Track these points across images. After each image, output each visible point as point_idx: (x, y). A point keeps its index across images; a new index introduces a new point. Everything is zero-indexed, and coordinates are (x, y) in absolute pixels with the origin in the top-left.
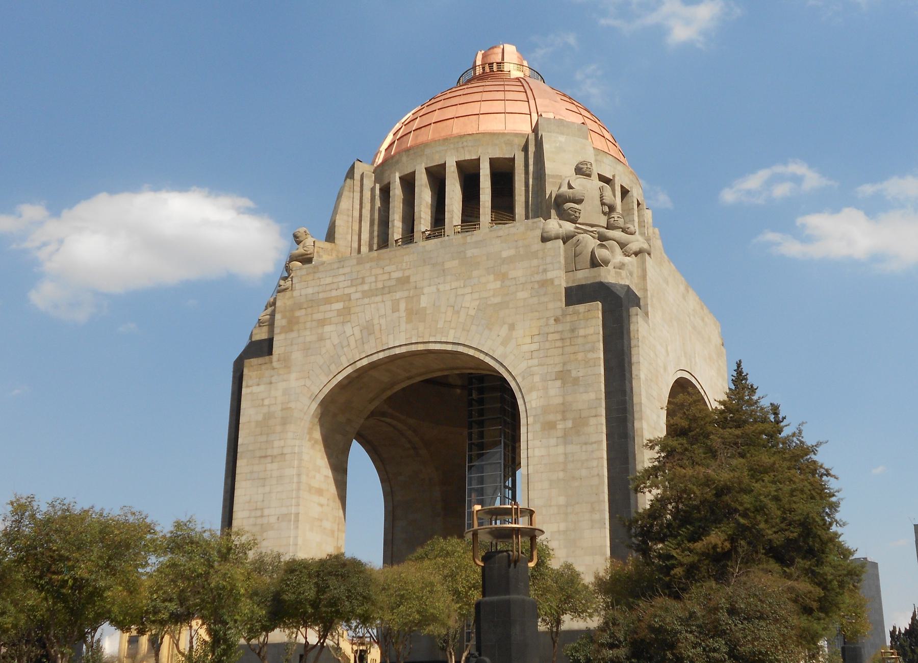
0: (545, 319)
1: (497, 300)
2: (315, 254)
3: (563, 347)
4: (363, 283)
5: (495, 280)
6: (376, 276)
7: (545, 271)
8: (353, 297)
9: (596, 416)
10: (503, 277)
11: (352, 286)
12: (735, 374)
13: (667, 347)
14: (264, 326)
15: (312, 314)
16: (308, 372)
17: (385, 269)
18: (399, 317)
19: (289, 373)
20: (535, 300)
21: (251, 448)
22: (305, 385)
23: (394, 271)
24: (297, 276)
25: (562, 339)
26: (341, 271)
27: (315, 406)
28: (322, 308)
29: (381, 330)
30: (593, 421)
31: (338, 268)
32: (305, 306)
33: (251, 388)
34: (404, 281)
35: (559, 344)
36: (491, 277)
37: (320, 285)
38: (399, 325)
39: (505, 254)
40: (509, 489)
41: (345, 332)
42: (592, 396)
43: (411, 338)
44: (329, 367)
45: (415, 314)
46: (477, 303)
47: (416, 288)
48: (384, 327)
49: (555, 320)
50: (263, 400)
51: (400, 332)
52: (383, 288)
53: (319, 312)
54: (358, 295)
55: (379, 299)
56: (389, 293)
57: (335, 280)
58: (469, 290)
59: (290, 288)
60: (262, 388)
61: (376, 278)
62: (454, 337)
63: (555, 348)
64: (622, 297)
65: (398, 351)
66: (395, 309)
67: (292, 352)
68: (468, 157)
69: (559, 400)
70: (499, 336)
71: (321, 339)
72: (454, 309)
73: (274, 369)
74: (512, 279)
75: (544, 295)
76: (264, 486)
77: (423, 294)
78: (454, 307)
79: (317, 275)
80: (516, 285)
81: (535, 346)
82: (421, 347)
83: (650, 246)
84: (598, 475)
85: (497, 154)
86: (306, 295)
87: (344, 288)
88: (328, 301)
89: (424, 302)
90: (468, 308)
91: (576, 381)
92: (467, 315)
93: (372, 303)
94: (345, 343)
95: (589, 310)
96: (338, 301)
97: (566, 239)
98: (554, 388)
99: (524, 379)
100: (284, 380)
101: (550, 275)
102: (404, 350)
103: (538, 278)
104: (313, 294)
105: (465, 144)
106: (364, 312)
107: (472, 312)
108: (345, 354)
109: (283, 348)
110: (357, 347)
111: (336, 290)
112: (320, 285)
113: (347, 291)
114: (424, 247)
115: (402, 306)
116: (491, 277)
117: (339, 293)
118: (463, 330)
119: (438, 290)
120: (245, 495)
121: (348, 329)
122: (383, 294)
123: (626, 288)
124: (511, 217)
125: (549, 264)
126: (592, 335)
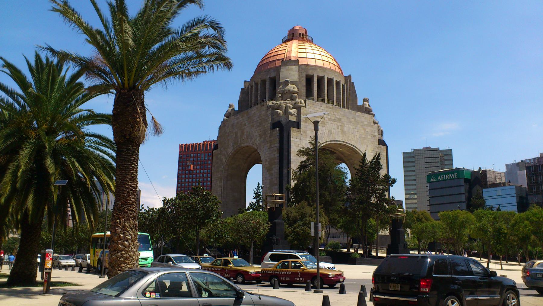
5: (363, 130)
10: (365, 130)
17: (335, 113)
18: (339, 131)
19: (307, 138)
20: (372, 140)
21: (295, 161)
26: (321, 108)
34: (340, 120)
45: (343, 132)
50: (298, 145)
52: (334, 119)
55: (333, 122)
73: (301, 134)
75: (374, 139)
79: (314, 106)
89: (346, 129)
94: (324, 134)
107: (358, 138)
112: (315, 110)
115: (340, 128)
116: (362, 129)
118: (356, 142)
119: (349, 127)
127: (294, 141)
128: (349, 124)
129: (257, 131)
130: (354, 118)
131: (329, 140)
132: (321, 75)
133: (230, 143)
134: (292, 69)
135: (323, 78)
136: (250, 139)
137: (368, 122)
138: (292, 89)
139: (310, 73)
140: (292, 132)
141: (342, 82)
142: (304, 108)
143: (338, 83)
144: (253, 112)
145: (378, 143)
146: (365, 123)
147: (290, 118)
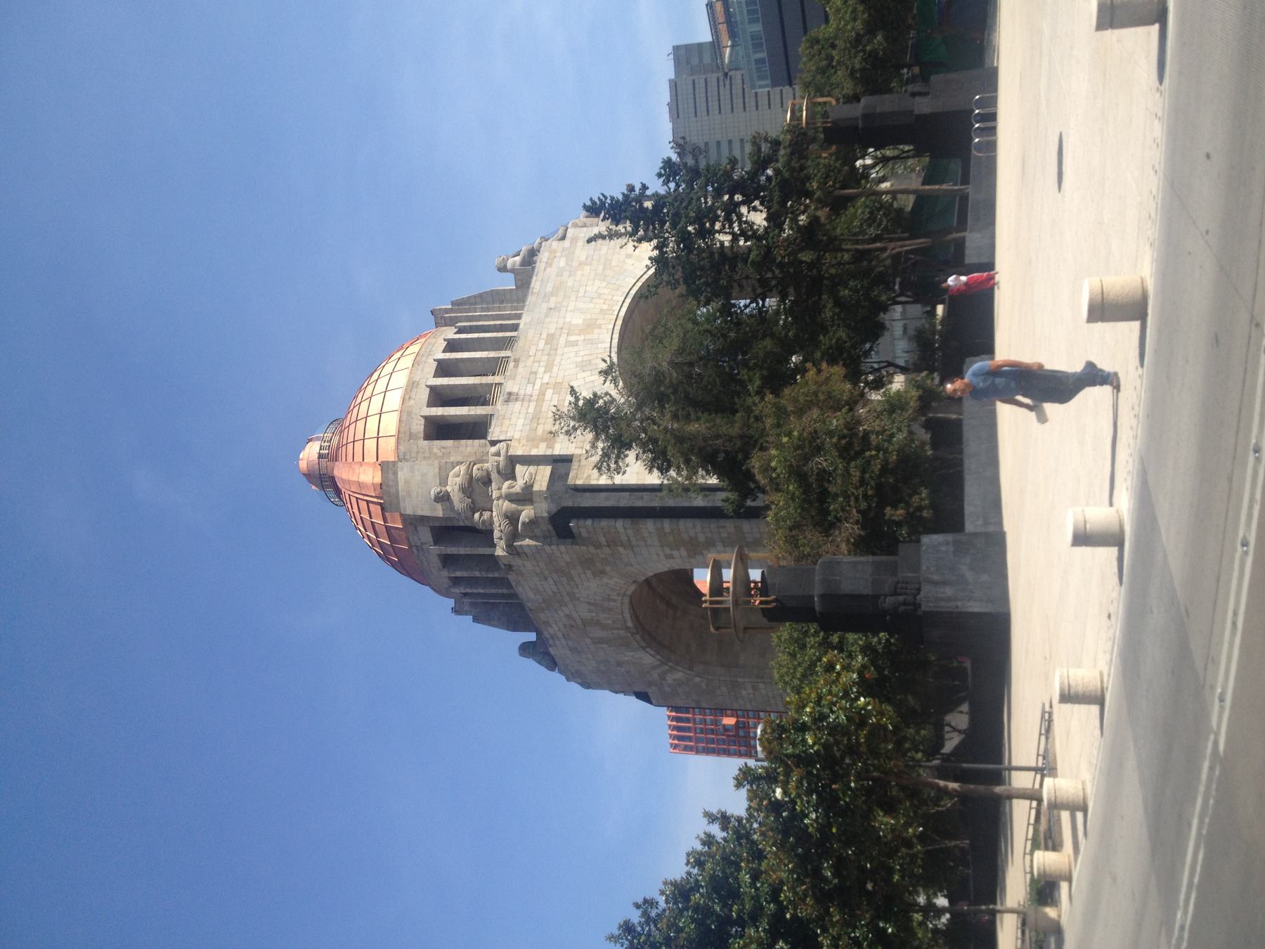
4: (535, 373)
8: (546, 379)
28: (544, 409)
37: (520, 413)
47: (562, 328)
48: (588, 352)
52: (549, 354)
55: (558, 359)
58: (582, 290)
59: (509, 442)
61: (537, 362)
65: (615, 341)
82: (619, 322)
96: (544, 395)
102: (616, 336)
107: (604, 284)
112: (520, 413)
113: (537, 386)
118: (617, 290)
119: (572, 311)
128: (563, 312)
129: (585, 583)
130: (547, 297)
132: (424, 394)
133: (626, 659)
134: (407, 482)
135: (434, 390)
136: (611, 603)
137: (561, 256)
138: (458, 480)
139: (419, 426)
140: (579, 482)
141: (450, 333)
142: (512, 443)
143: (452, 346)
144: (531, 595)
146: (562, 263)
147: (541, 486)
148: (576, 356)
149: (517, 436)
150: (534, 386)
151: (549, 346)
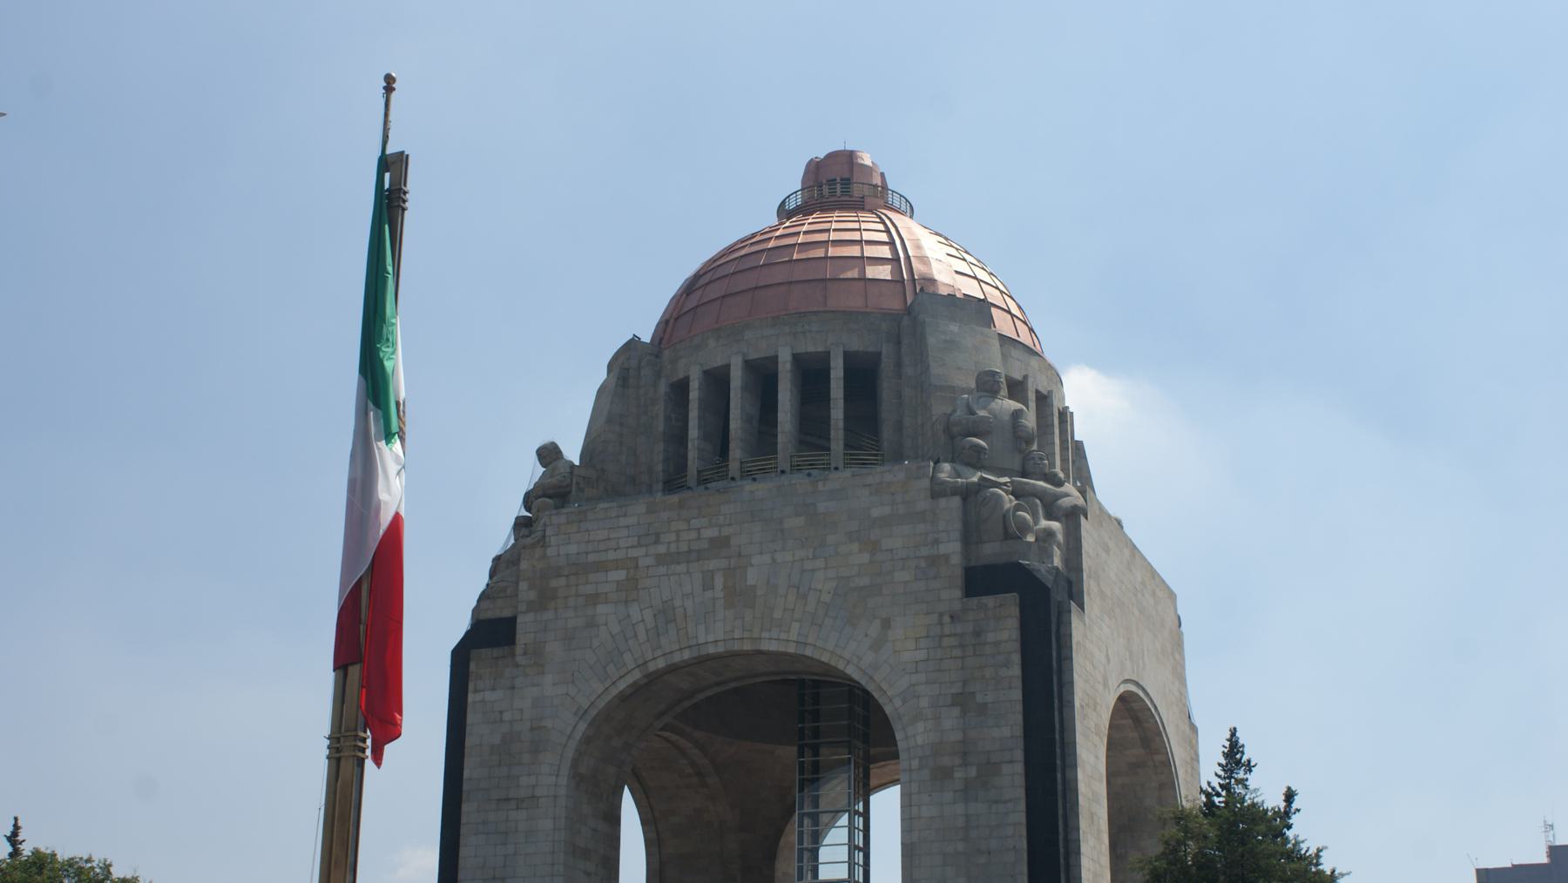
0: (936, 615)
1: (864, 581)
2: (574, 489)
3: (963, 658)
4: (657, 542)
5: (860, 551)
6: (678, 532)
7: (936, 542)
8: (642, 562)
9: (1011, 762)
11: (639, 545)
12: (1227, 744)
13: (1107, 651)
14: (499, 598)
15: (577, 585)
16: (573, 675)
17: (693, 521)
18: (714, 599)
22: (567, 694)
23: (705, 528)
24: (551, 525)
25: (962, 646)
26: (623, 522)
27: (582, 726)
28: (592, 577)
29: (686, 616)
30: (1006, 769)
31: (618, 517)
32: (566, 573)
33: (482, 693)
34: (721, 543)
35: (957, 652)
36: (855, 547)
37: (588, 542)
38: (714, 612)
39: (875, 513)
40: (860, 849)
41: (629, 616)
42: (1006, 732)
43: (733, 631)
44: (604, 668)
46: (834, 584)
47: (740, 555)
49: (952, 617)
50: (501, 712)
51: (715, 621)
52: (690, 551)
53: (587, 583)
54: (650, 561)
55: (681, 568)
56: (699, 561)
57: (612, 536)
58: (820, 563)
60: (498, 694)
62: (799, 634)
63: (951, 658)
64: (1050, 586)
65: (712, 650)
66: (708, 585)
67: (545, 642)
68: (811, 349)
69: (959, 736)
70: (866, 636)
71: (591, 624)
72: (798, 593)
74: (887, 550)
76: (505, 844)
77: (752, 565)
78: (798, 588)
80: (893, 560)
81: (922, 655)
82: (747, 646)
83: (1086, 501)
84: (1015, 847)
85: (856, 345)
86: (567, 555)
87: (627, 548)
88: (602, 567)
89: (752, 577)
90: (820, 591)
91: (983, 709)
92: (819, 601)
93: (672, 575)
95: (1001, 606)
96: (617, 569)
97: (969, 494)
98: (950, 719)
99: (904, 701)
100: (534, 685)
101: (944, 549)
102: (721, 649)
103: (925, 551)
104: (578, 554)
105: (807, 327)
106: (659, 587)
107: (826, 598)
108: (630, 651)
109: (532, 635)
110: (648, 640)
111: (615, 550)
113: (633, 553)
114: (752, 492)
115: (719, 581)
117: (620, 554)
119: (774, 560)
120: (476, 856)
121: (634, 611)
122: (688, 562)
123: (1054, 571)
124: (873, 440)
125: (943, 531)
126: (1006, 642)
127: (483, 701)
131: (659, 653)
132: (718, 361)
140: (473, 666)
142: (538, 552)
145: (958, 593)
148: (683, 595)
149: (550, 552)
150: (632, 547)
151: (706, 546)
